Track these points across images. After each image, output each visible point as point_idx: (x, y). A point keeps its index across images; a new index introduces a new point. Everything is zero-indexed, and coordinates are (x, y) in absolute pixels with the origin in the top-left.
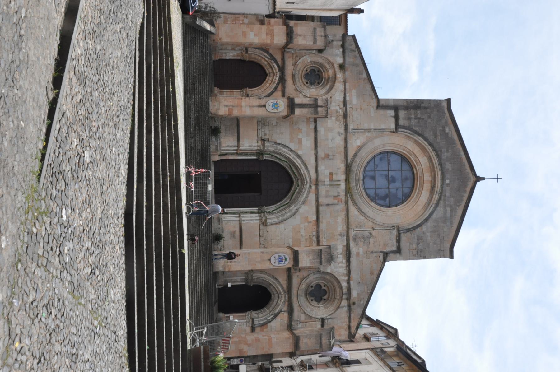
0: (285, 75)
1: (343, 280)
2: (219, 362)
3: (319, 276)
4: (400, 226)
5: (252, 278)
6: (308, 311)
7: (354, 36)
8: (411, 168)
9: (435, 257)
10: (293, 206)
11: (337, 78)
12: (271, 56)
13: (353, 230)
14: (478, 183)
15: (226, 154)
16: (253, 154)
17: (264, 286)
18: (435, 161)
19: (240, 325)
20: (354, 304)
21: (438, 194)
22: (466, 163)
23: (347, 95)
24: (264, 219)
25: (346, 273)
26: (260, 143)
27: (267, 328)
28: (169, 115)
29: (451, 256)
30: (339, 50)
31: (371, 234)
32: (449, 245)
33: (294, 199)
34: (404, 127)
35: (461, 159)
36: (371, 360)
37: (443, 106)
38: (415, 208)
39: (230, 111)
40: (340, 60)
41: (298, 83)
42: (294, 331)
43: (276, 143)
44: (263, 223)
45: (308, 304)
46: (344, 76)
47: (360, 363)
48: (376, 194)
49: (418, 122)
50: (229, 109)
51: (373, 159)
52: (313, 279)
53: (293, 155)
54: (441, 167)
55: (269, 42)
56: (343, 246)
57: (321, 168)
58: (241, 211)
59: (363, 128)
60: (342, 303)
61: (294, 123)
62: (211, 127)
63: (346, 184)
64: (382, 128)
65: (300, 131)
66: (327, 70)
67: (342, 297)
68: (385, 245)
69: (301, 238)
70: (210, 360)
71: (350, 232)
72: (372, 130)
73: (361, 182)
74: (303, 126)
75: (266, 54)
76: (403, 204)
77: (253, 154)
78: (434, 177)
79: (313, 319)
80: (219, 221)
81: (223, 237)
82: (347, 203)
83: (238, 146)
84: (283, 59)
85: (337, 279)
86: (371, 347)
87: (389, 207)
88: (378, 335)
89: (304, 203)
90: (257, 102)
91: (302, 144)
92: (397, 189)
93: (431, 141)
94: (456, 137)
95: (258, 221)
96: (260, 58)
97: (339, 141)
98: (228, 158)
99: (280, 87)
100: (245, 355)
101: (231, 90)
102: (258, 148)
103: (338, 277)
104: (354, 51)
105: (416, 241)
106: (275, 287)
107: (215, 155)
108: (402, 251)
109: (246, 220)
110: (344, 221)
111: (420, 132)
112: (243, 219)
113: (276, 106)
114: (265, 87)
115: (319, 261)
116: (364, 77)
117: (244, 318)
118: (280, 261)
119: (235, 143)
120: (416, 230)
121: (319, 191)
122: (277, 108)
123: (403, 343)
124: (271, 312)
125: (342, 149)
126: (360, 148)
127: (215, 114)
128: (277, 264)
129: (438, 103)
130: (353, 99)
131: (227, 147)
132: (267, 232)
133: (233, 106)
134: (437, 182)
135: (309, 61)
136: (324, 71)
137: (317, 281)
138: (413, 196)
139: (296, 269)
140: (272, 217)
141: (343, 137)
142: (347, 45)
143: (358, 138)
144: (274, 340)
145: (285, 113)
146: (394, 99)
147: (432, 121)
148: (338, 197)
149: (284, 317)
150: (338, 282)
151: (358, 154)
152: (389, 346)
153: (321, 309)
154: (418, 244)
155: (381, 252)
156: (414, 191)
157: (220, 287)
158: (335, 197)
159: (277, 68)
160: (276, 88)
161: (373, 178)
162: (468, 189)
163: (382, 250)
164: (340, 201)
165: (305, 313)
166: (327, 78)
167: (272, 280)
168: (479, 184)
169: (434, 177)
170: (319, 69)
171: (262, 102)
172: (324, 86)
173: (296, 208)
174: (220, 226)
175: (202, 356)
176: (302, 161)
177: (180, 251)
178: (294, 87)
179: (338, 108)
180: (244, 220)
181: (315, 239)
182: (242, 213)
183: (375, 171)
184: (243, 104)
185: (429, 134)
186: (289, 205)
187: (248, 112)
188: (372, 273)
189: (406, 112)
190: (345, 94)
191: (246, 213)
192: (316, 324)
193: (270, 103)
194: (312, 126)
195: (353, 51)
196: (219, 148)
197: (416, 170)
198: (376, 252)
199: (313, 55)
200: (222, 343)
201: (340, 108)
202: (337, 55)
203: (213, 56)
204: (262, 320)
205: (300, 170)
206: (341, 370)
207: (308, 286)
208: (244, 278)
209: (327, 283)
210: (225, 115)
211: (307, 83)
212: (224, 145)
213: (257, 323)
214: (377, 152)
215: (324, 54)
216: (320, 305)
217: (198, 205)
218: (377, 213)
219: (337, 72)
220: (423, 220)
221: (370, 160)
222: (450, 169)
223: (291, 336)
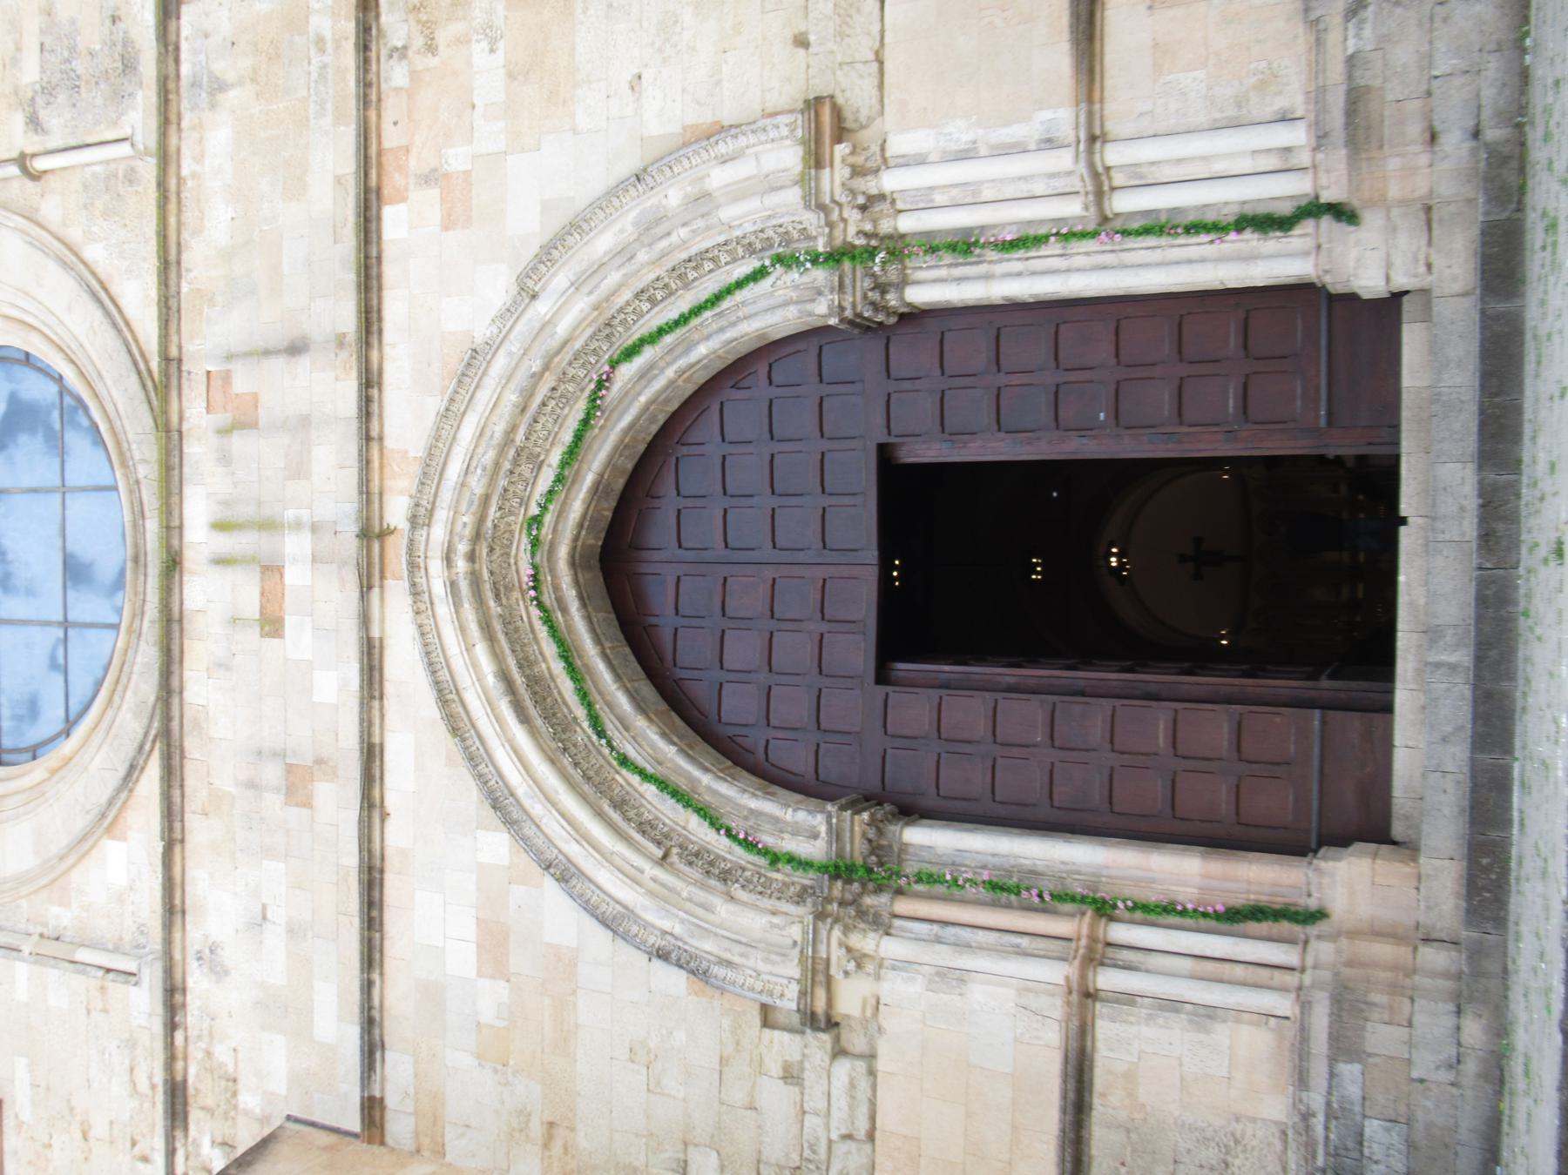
10: (562, 329)
13: (138, 138)
15: (1236, 917)
24: (833, 180)
26: (850, 997)
31: (34, 123)
43: (697, 970)
51: (72, 717)
53: (554, 827)
59: (78, 982)
61: (536, 1128)
71: (153, 123)
72: (26, 949)
89: (475, 360)
107: (1377, 933)
109: (1017, 149)
110: (189, 216)
121: (351, 476)
125: (199, 831)
126: (107, 820)
132: (802, 42)
141: (196, 932)
158: (243, 421)
161: (75, 571)
173: (542, 308)
174: (1342, 41)
176: (475, 758)
180: (1049, 143)
182: (1070, 235)
183: (66, 624)
191: (1024, 242)
212: (1256, 1043)
214: (37, 771)
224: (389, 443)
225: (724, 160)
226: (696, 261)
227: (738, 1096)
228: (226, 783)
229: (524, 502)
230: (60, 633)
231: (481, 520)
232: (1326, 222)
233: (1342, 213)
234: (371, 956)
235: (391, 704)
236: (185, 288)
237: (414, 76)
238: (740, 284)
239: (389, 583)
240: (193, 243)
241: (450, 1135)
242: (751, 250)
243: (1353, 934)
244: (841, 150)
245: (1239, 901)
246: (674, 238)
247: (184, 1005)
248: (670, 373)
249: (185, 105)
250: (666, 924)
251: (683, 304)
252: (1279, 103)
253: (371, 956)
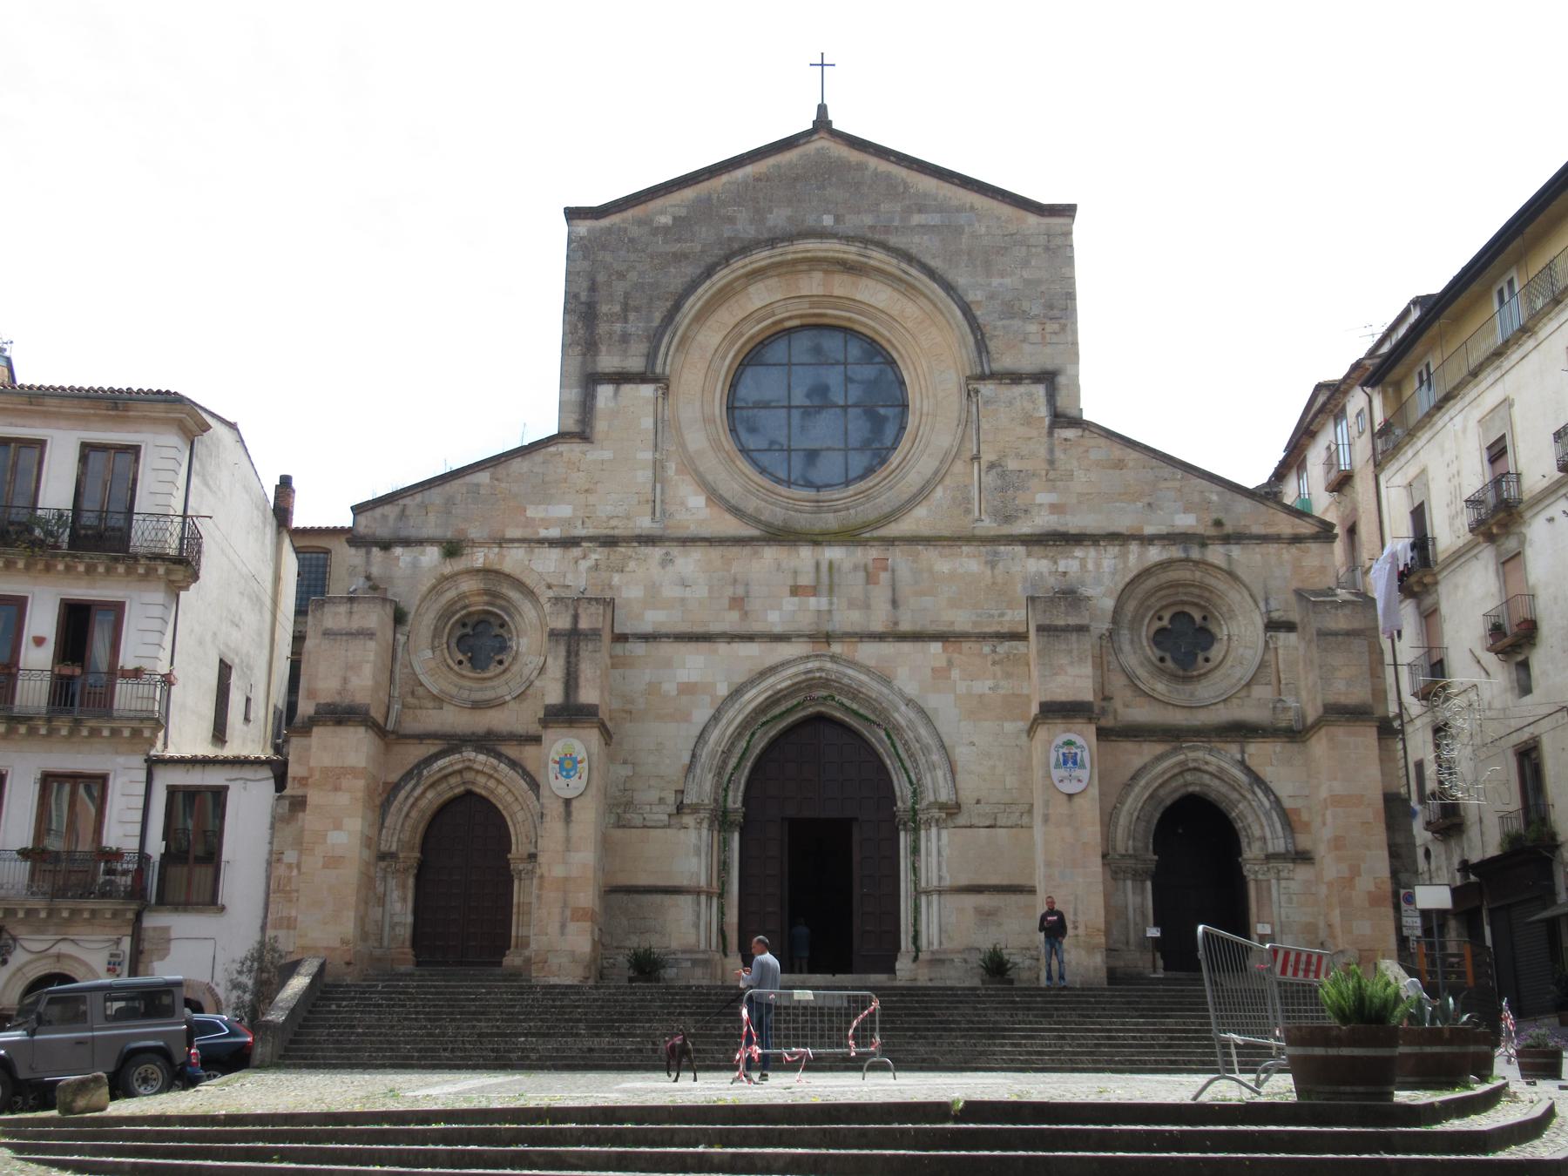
0: (473, 734)
1: (1140, 556)
2: (1341, 993)
3: (1125, 634)
4: (968, 373)
5: (1130, 856)
6: (1242, 673)
7: (358, 510)
8: (784, 332)
9: (1070, 261)
10: (896, 715)
11: (488, 566)
12: (408, 776)
14: (835, 126)
15: (722, 933)
16: (724, 845)
17: (1157, 815)
18: (761, 257)
19: (1290, 901)
20: (1218, 523)
21: (869, 252)
22: (771, 161)
23: (543, 533)
24: (935, 813)
25: (1117, 548)
26: (688, 820)
27: (1297, 811)
28: (517, 1137)
29: (1068, 211)
30: (398, 558)
31: (992, 466)
32: (1032, 219)
33: (874, 710)
34: (651, 357)
35: (757, 179)
36: (1412, 471)
37: (588, 231)
38: (909, 325)
39: (579, 915)
40: (431, 555)
41: (500, 692)
42: (1310, 720)
43: (690, 767)
44: (950, 815)
45: (1218, 674)
46: (481, 544)
47: (1422, 504)
48: (864, 446)
49: (637, 309)
50: (572, 920)
51: (750, 453)
52: (1136, 655)
53: (731, 713)
54: (782, 240)
55: (361, 783)
56: (1029, 555)
57: (774, 620)
58: (911, 886)
59: (649, 487)
60: (1217, 562)
61: (628, 707)
62: (631, 980)
63: (830, 544)
64: (651, 426)
65: (653, 689)
66: (462, 596)
67: (1196, 563)
68: (1028, 420)
69: (1002, 692)
70: (1333, 1022)
72: (658, 456)
73: (825, 494)
74: (640, 678)
75: (402, 795)
76: (899, 362)
77: (724, 845)
78: (814, 263)
79: (1270, 656)
80: (942, 961)
81: (994, 949)
82: (891, 542)
83: (697, 892)
84: (421, 737)
85: (1139, 576)
86: (1371, 467)
87: (905, 406)
88: (1333, 447)
89: (886, 681)
90: (554, 828)
91: (696, 684)
92: (848, 379)
93: (699, 271)
94: (689, 193)
95: (944, 833)
96: (414, 814)
97: (689, 562)
98: (735, 927)
99: (511, 751)
100: (1388, 887)
101: (515, 910)
102: (705, 825)
103: (1131, 575)
104: (403, 511)
105: (1016, 323)
106: (1160, 781)
108: (1050, 367)
109: (939, 870)
110: (947, 551)
111: (669, 304)
112: (935, 883)
113: (568, 764)
114: (509, 799)
115: (1074, 637)
116: (487, 480)
117: (1265, 884)
118: (1075, 763)
119: (686, 901)
120: (980, 321)
121: (848, 629)
122: (577, 762)
123: (1357, 366)
124: (1244, 797)
125: (715, 553)
126: (714, 497)
127: (588, 967)
128: (1084, 774)
129: (577, 249)
130: (557, 515)
131: (697, 926)
132: (978, 802)
133: (565, 905)
134: (831, 254)
135: (429, 654)
136: (465, 607)
137: (1145, 643)
138: (873, 329)
139: (1104, 711)
140: (930, 785)
141: (675, 551)
142: (383, 532)
143: (683, 504)
144: (1338, 787)
145: (594, 735)
146: (561, 387)
147: (634, 268)
148: (871, 570)
149: (1260, 753)
150: (1146, 573)
151: (733, 502)
152: (1366, 411)
153: (1235, 630)
154: (1026, 316)
155: (1050, 433)
156: (857, 327)
157: (1160, 963)
158: (870, 579)
160: (513, 764)
161: (812, 456)
162: (855, 156)
163: (1045, 431)
164: (882, 564)
165: (1248, 685)
166: (486, 598)
167: (1137, 789)
168: (838, 124)
169: (814, 263)
170: (457, 622)
171: (555, 809)
172: (510, 607)
173: (903, 708)
174: (957, 959)
175: (1319, 1051)
177: (957, 1119)
178: (512, 705)
179: (584, 565)
180: (940, 878)
181: (1004, 647)
182: (916, 883)
183: (789, 450)
184: (558, 871)
185: (676, 278)
186: (892, 731)
187: (585, 857)
188: (1119, 465)
189: (603, 348)
190: (541, 542)
191: (915, 870)
192: (1286, 647)
193: (558, 785)
194: (639, 649)
195: (403, 514)
196: (700, 956)
197: (790, 318)
198: (1051, 451)
199: (412, 643)
200: (1295, 973)
201: (584, 558)
202: (415, 565)
203: (402, 969)
204: (1272, 826)
205: (781, 690)
206: (1443, 569)
207: (1160, 671)
208: (1129, 883)
209: (1149, 608)
210: (592, 932)
211: (501, 662)
213: (1282, 841)
214: (728, 443)
215: (411, 604)
216: (1222, 633)
217: (862, 1036)
218: (927, 446)
219: (469, 565)
220: (949, 301)
221: (755, 463)
222: (788, 212)
223: (1323, 731)
224: (859, 645)
225: (945, 775)
226: (916, 760)
227: (652, 782)
228: (736, 568)
229: (840, 694)
230: (785, 447)
231: (833, 680)
232: (914, 954)
233: (916, 959)
234: (681, 637)
235: (769, 645)
236: (920, 548)
237: (986, 655)
238: (909, 777)
239: (811, 645)
240: (937, 552)
241: (621, 671)
242: (919, 780)
243: (723, 965)
244: (944, 815)
245: (727, 933)
246: (922, 757)
247: (647, 546)
248: (882, 750)
249: (989, 548)
250: (704, 756)
251: (903, 755)
252: (944, 941)
253: (681, 637)
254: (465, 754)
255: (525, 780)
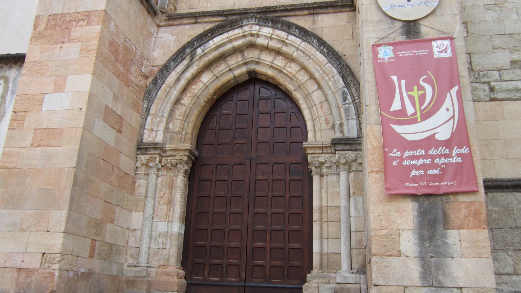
96: (186, 100)
159: (225, 35)
254: (246, 28)
255: (322, 52)
